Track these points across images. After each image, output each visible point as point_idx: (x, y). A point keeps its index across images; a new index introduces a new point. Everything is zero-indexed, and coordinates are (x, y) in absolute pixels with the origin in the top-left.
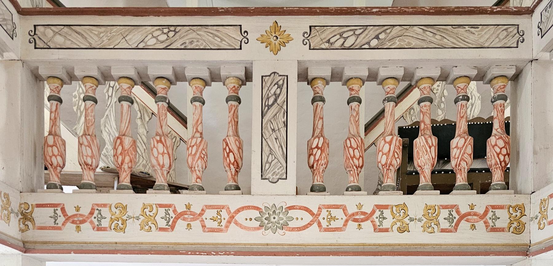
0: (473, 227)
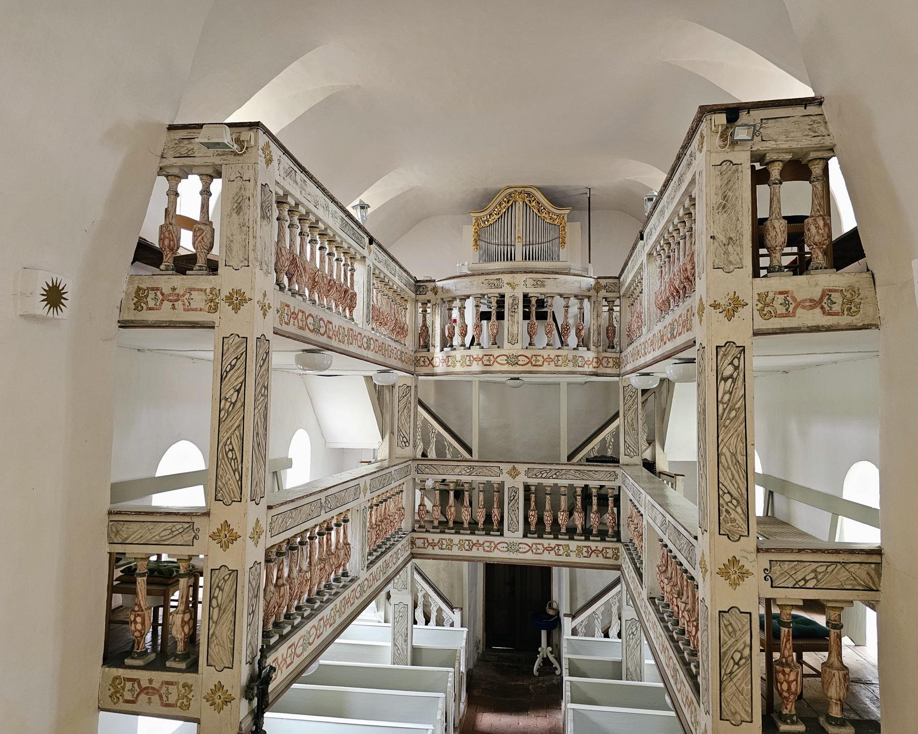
0: (597, 556)
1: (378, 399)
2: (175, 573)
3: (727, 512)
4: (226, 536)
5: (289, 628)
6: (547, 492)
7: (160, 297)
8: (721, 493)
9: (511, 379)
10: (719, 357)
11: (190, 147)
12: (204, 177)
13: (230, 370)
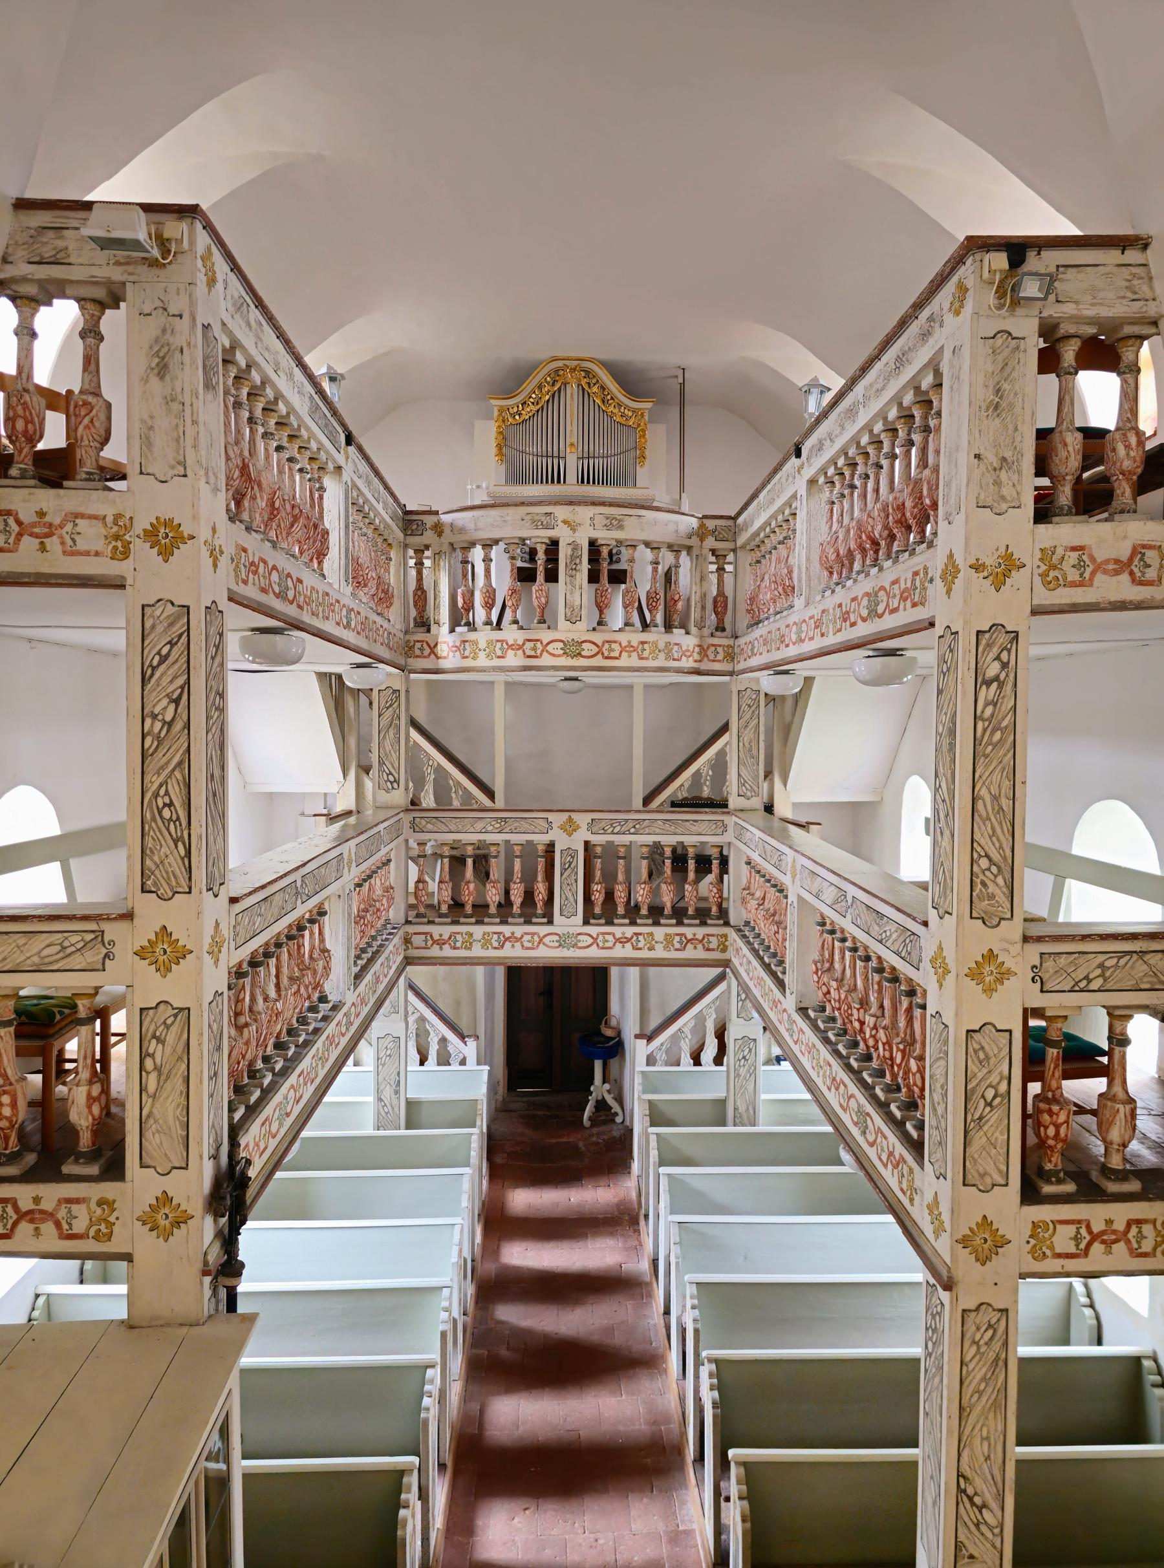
0: (695, 948)
1: (336, 709)
2: (58, 1017)
3: (984, 884)
4: (165, 952)
5: (257, 1094)
6: (621, 854)
7: (15, 528)
8: (975, 856)
9: (566, 679)
10: (981, 649)
11: (61, 244)
12: (89, 305)
13: (159, 664)
